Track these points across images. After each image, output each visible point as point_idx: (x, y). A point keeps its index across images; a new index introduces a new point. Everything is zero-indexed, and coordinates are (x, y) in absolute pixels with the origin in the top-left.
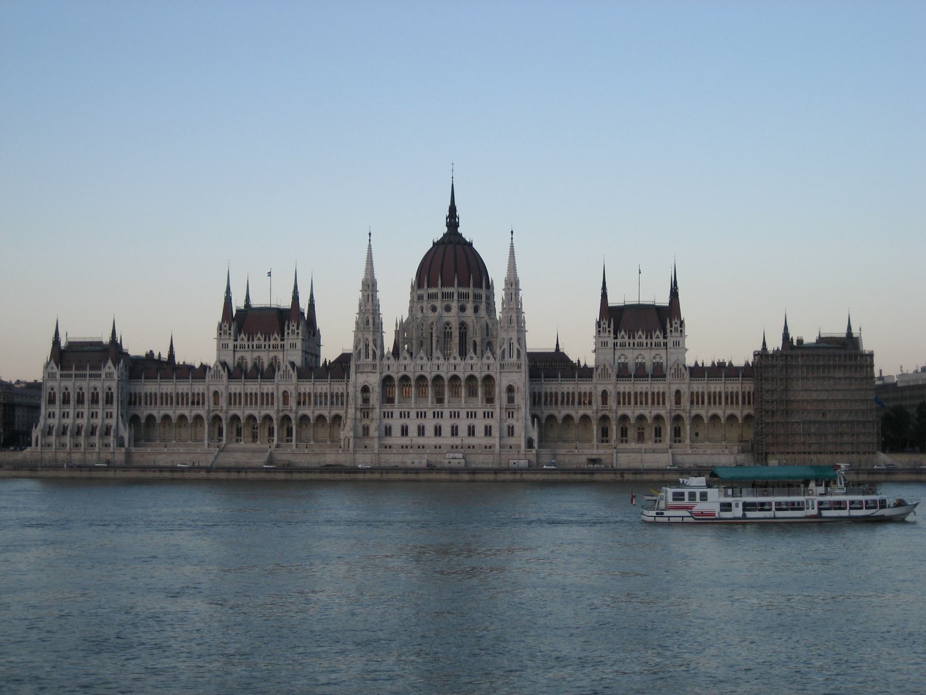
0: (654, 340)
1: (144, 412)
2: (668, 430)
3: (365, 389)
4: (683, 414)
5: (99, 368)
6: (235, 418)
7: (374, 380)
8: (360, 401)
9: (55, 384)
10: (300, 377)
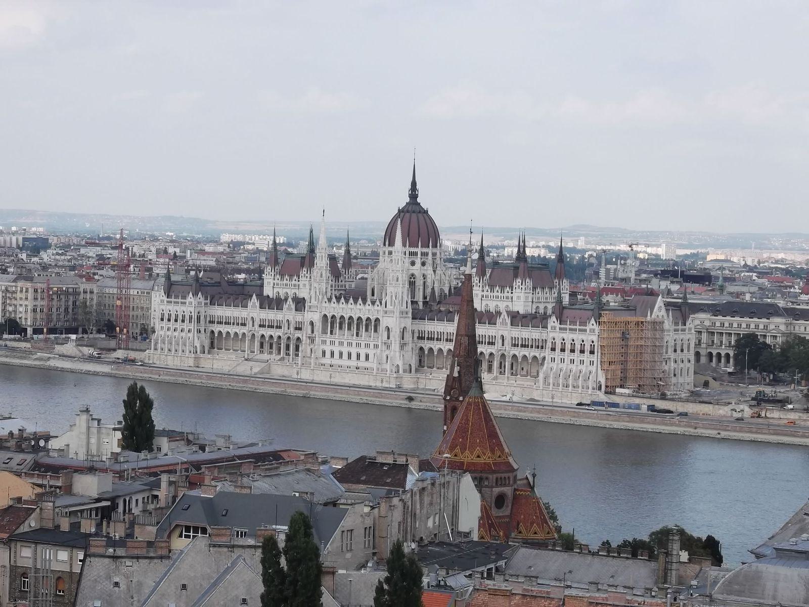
0: (506, 294)
1: (217, 328)
2: (496, 364)
3: (312, 324)
4: (506, 354)
5: (184, 297)
6: (263, 336)
7: (316, 317)
8: (309, 332)
9: (163, 307)
10: (296, 310)
